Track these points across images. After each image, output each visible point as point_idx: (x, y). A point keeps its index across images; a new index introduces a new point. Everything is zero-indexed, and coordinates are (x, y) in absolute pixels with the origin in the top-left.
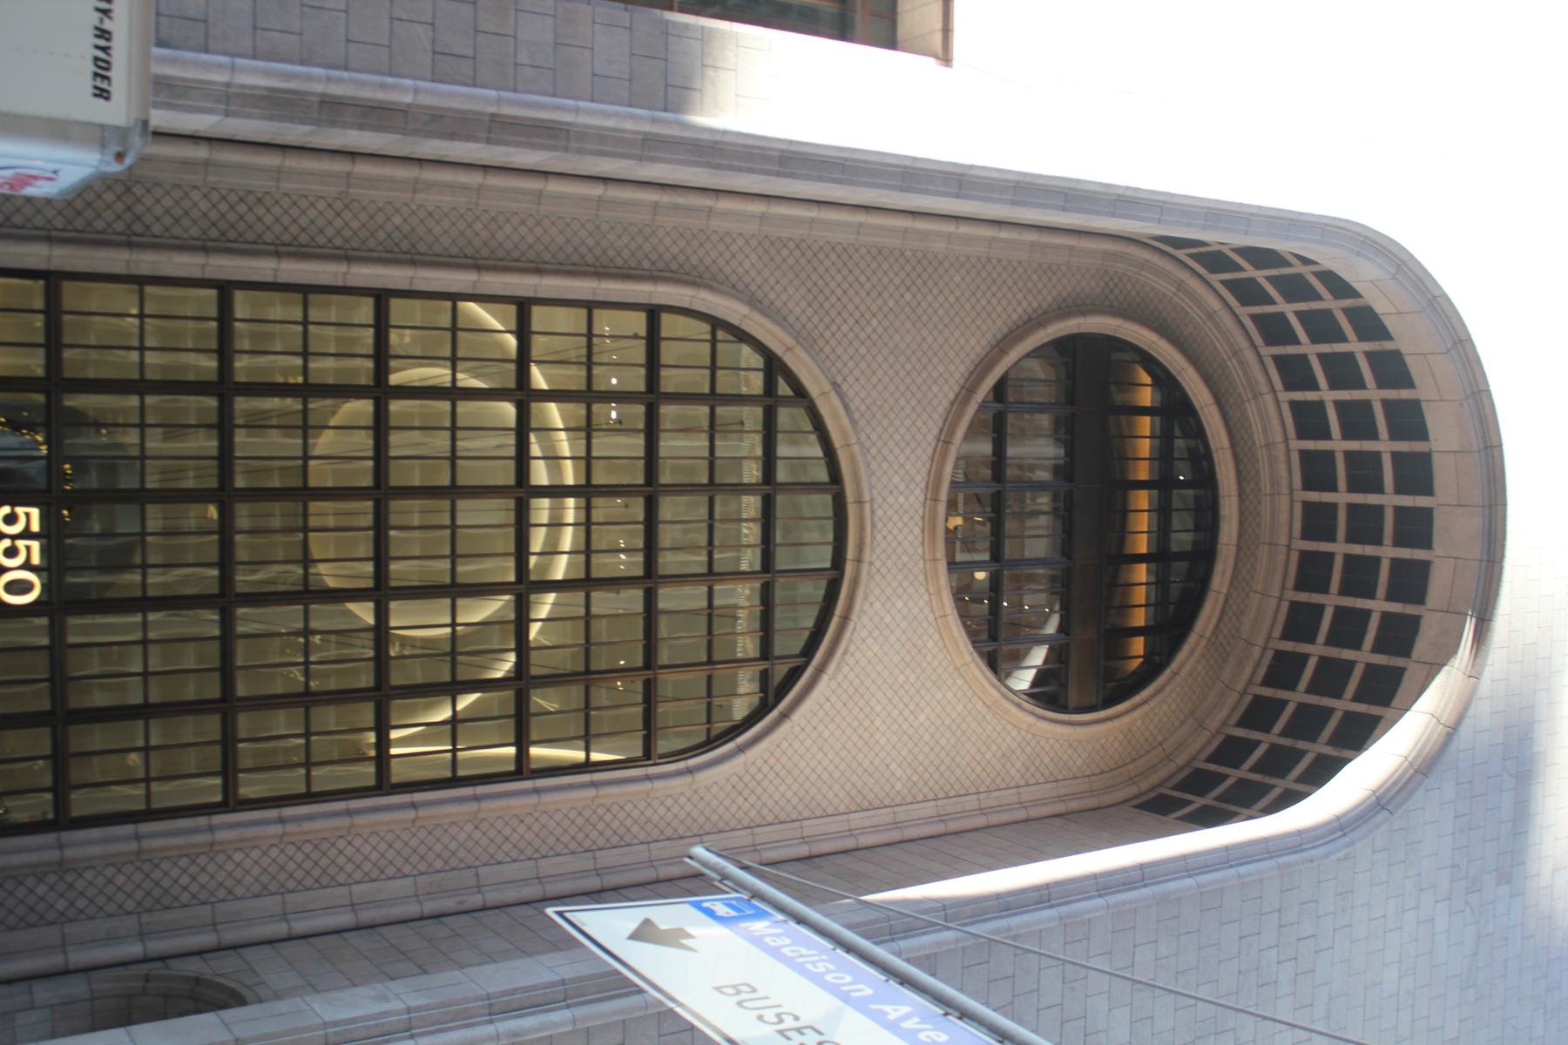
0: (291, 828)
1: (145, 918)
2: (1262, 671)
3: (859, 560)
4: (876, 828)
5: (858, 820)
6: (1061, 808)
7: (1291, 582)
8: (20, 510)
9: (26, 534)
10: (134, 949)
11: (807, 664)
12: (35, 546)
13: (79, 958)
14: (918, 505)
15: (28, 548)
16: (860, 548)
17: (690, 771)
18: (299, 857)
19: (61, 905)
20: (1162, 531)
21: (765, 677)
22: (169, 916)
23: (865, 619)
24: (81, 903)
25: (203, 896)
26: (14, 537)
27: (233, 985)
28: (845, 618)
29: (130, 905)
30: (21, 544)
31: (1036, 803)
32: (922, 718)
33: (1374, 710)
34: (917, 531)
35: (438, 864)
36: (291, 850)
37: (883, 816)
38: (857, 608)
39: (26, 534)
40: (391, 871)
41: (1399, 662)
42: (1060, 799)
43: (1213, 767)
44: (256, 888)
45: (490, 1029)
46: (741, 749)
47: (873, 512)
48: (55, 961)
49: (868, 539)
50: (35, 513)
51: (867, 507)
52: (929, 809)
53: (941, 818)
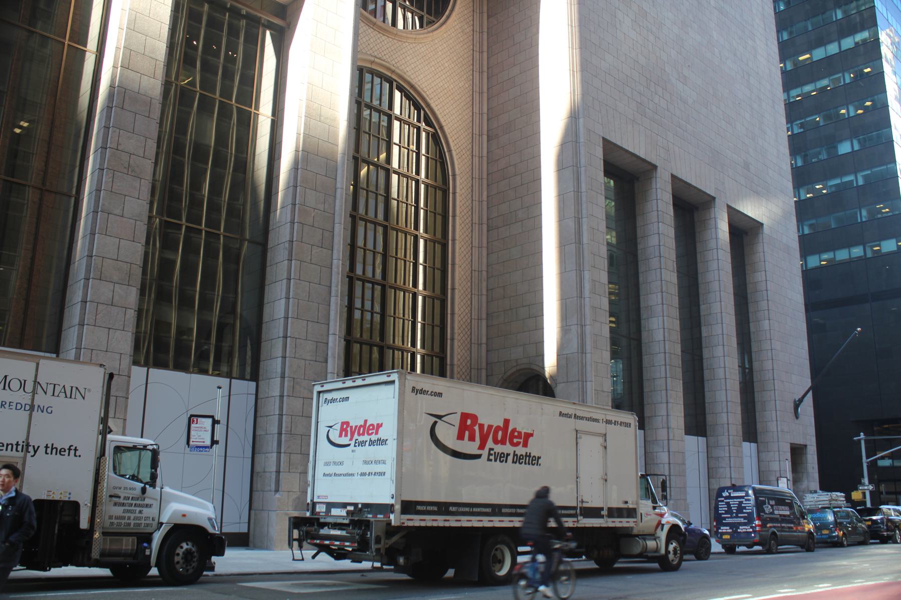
0: (456, 336)
3: (393, 72)
4: (481, 102)
5: (476, 110)
6: (485, 15)
11: (424, 110)
16: (388, 69)
17: (454, 175)
23: (412, 77)
25: (468, 371)
28: (412, 86)
31: (481, 26)
32: (446, 65)
35: (469, 284)
37: (476, 96)
38: (409, 79)
42: (481, 13)
44: (468, 352)
45: (587, 300)
46: (450, 151)
47: (380, 59)
49: (387, 65)
51: (376, 60)
52: (477, 75)
53: (481, 72)
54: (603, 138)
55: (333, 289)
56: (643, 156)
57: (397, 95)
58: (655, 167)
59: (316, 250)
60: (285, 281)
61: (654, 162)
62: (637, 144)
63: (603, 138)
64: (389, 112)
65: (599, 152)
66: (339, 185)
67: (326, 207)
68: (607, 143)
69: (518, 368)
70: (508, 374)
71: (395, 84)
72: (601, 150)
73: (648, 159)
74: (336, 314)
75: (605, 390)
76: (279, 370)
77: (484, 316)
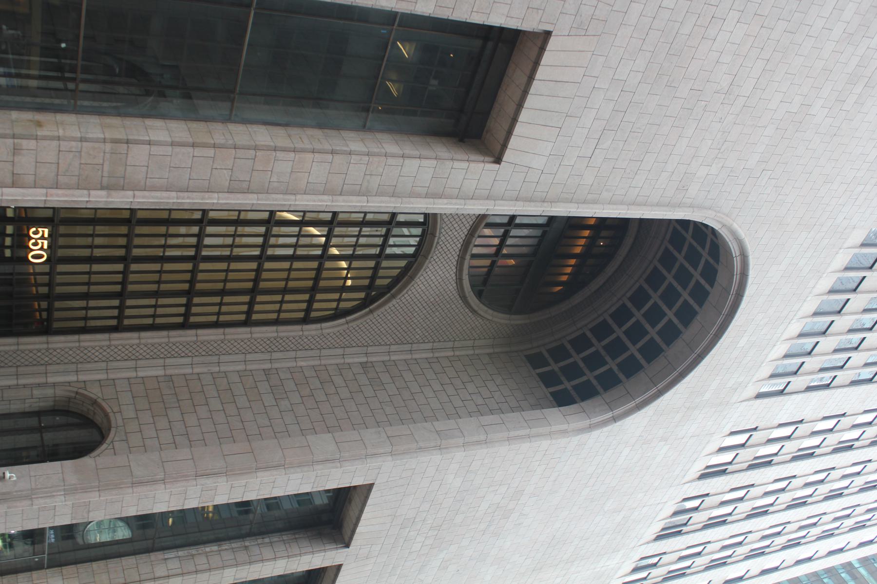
1: (79, 366)
2: (614, 309)
7: (644, 276)
8: (40, 230)
9: (42, 238)
10: (72, 378)
11: (389, 292)
12: (46, 242)
13: (51, 380)
14: (463, 236)
15: (43, 243)
18: (145, 349)
19: (47, 359)
20: (588, 247)
21: (367, 295)
22: (88, 366)
23: (422, 278)
24: (55, 359)
26: (36, 239)
27: (109, 410)
29: (74, 360)
30: (39, 241)
33: (643, 362)
34: (459, 245)
36: (142, 346)
39: (42, 238)
40: (183, 354)
41: (664, 346)
43: (569, 347)
48: (42, 380)
50: (46, 231)
54: (373, 484)
55: (186, 194)
56: (359, 530)
57: (402, 263)
58: (347, 546)
59: (227, 174)
60: (191, 140)
61: (353, 543)
62: (370, 522)
63: (373, 484)
64: (383, 256)
65: (357, 481)
66: (299, 197)
67: (275, 184)
68: (370, 486)
69: (111, 415)
70: (104, 404)
71: (412, 259)
72: (361, 484)
73: (356, 537)
74: (157, 198)
75: (91, 514)
76: (90, 135)
77: (169, 372)
